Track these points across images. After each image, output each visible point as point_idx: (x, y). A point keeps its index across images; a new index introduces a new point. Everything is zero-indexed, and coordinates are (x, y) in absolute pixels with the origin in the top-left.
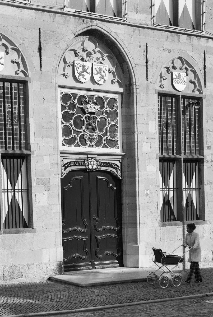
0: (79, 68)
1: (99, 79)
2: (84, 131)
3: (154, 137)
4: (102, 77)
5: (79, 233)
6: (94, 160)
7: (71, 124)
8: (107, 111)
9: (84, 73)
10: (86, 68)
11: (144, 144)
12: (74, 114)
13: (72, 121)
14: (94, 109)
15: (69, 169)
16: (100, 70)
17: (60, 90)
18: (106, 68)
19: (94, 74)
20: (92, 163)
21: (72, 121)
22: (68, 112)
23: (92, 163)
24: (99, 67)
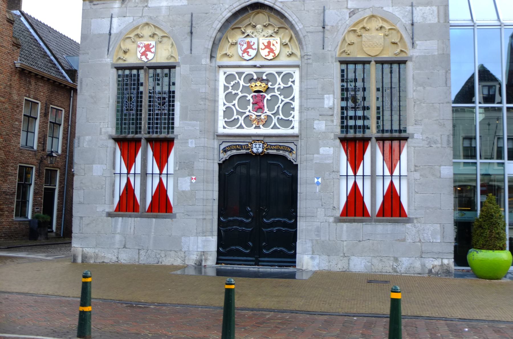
0: (243, 45)
1: (268, 54)
2: (249, 111)
3: (331, 113)
4: (272, 51)
5: (241, 223)
6: (261, 142)
7: (234, 105)
8: (279, 89)
9: (249, 50)
10: (252, 44)
11: (316, 122)
12: (237, 94)
13: (236, 102)
14: (260, 87)
15: (229, 153)
16: (269, 43)
17: (222, 71)
18: (277, 41)
19: (260, 50)
20: (258, 146)
21: (236, 102)
22: (231, 92)
23: (258, 146)
24: (268, 40)
